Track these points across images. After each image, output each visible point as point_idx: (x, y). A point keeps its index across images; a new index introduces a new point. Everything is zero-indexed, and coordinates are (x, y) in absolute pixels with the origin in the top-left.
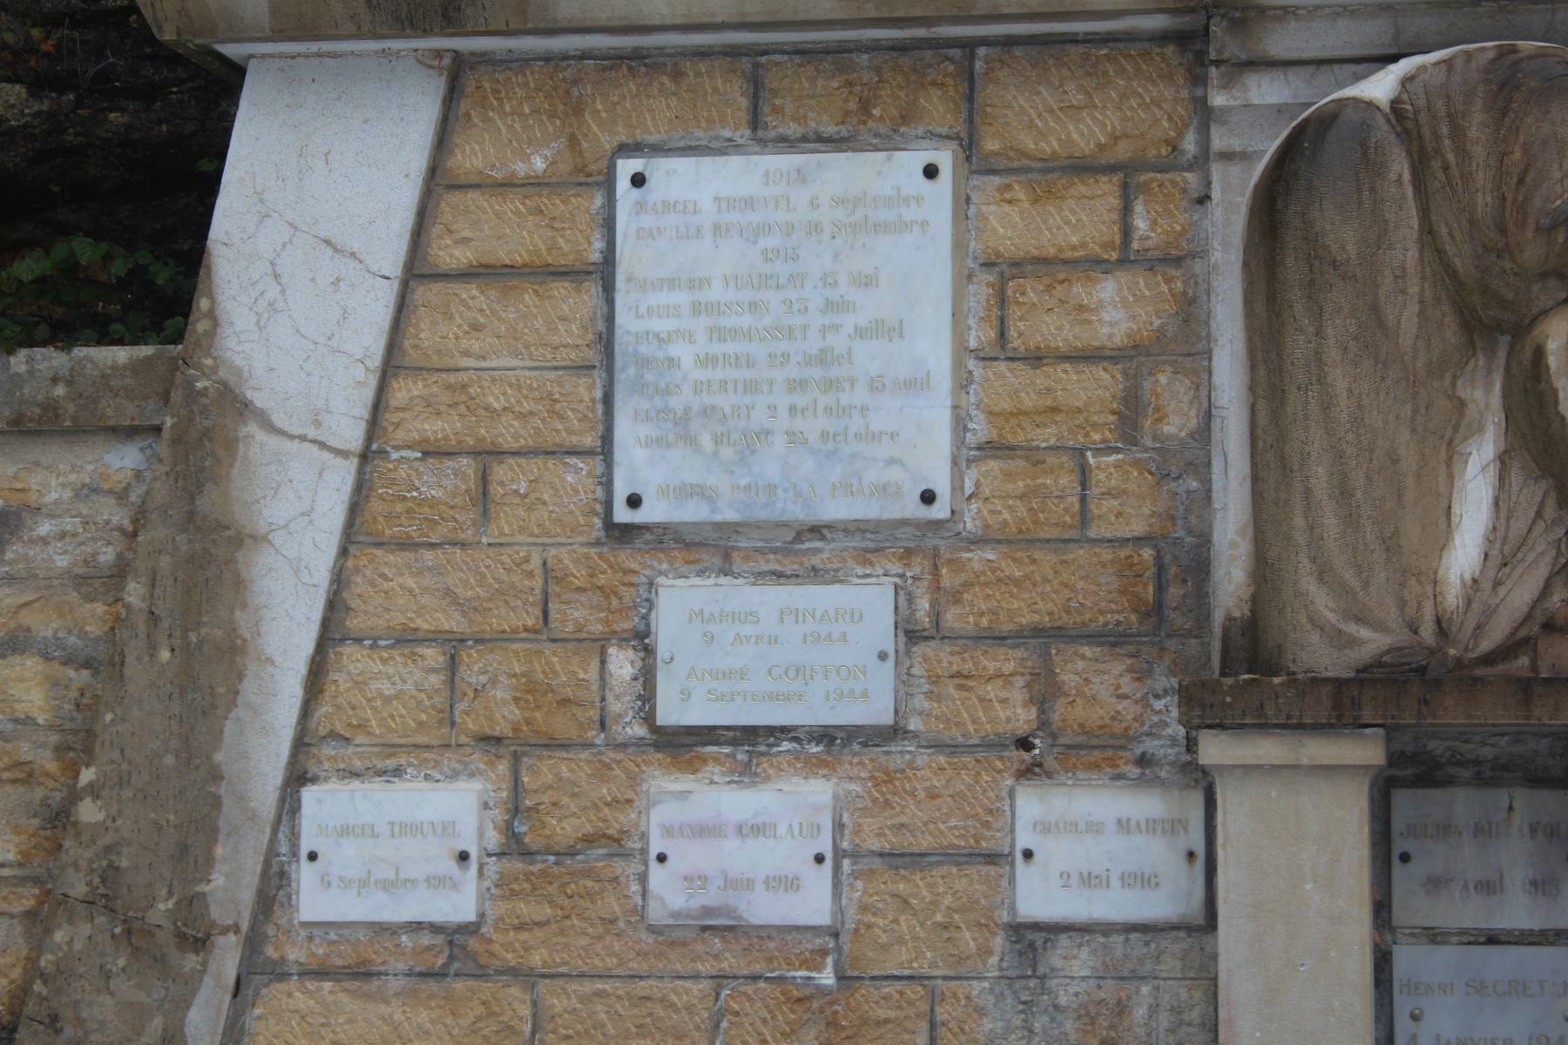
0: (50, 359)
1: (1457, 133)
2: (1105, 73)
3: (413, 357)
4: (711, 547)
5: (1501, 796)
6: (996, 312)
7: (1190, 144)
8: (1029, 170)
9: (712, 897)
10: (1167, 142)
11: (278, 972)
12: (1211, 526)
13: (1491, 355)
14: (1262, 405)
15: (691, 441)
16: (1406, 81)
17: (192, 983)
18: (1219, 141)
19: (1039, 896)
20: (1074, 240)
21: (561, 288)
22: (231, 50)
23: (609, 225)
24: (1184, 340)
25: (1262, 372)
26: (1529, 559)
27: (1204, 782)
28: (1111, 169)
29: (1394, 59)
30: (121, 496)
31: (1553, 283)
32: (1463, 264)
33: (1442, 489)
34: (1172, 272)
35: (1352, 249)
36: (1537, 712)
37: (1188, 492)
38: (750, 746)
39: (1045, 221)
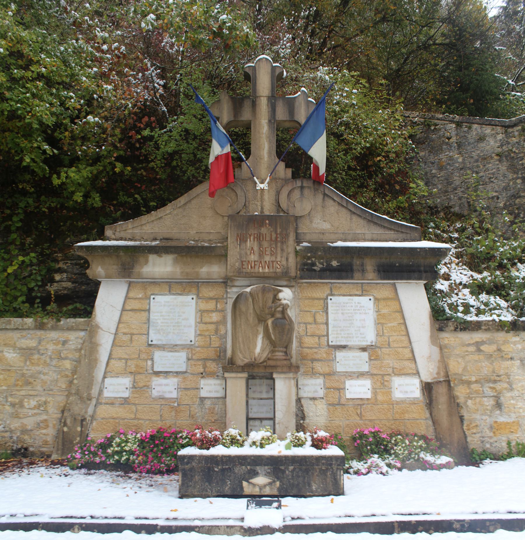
0: (72, 320)
1: (258, 296)
3: (122, 321)
4: (162, 347)
5: (262, 380)
7: (225, 296)
9: (160, 394)
11: (101, 404)
15: (160, 333)
17: (89, 405)
18: (229, 296)
19: (203, 393)
21: (143, 312)
22: (99, 280)
23: (149, 304)
24: (224, 321)
27: (225, 379)
30: (82, 339)
32: (258, 312)
38: (166, 374)
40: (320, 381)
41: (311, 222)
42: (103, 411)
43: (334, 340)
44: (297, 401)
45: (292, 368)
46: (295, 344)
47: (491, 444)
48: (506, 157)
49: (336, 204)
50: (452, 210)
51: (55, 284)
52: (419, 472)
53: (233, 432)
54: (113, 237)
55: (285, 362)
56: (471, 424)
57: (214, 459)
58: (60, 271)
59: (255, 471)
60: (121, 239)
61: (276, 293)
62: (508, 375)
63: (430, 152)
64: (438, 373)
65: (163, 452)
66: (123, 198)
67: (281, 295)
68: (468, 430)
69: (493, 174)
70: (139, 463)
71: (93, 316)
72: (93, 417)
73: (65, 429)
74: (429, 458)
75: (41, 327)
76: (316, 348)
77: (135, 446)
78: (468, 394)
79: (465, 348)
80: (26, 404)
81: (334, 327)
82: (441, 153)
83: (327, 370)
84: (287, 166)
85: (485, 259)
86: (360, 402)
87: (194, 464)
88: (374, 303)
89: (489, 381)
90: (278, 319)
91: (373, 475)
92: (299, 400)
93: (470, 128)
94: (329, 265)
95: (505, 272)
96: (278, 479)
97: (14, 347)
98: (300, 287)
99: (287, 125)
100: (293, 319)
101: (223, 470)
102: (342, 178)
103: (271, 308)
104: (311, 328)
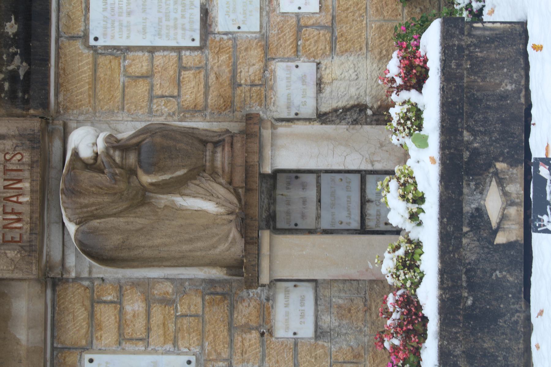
1: (86, 206)
2: (64, 308)
5: (279, 197)
6: (134, 341)
7: (86, 283)
8: (92, 331)
10: (85, 290)
12: (199, 279)
13: (152, 198)
14: (164, 264)
16: (70, 220)
18: (85, 275)
19: (307, 331)
20: (113, 318)
24: (145, 287)
25: (155, 264)
26: (211, 188)
27: (274, 282)
28: (92, 306)
29: (63, 224)
31: (131, 180)
32: (125, 205)
33: (190, 212)
34: (124, 288)
35: (119, 237)
36: (255, 187)
37: (189, 285)
39: (107, 326)
40: (280, 69)
43: (188, 35)
44: (323, 122)
45: (252, 130)
46: (199, 124)
53: (388, 264)
55: (238, 145)
57: (446, 308)
59: (472, 216)
61: (80, 164)
67: (86, 153)
76: (207, 77)
81: (159, 35)
83: (256, 54)
87: (458, 352)
90: (139, 161)
94: (15, 40)
96: (491, 165)
98: (66, 109)
101: (471, 287)
103: (114, 175)
104: (163, 86)
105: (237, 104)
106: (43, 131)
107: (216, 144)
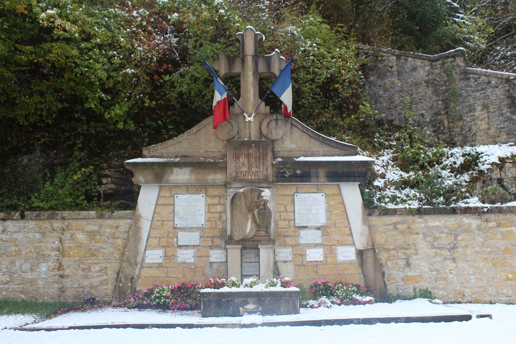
0: (122, 212)
4: (183, 229)
9: (183, 260)
11: (144, 267)
17: (136, 268)
18: (228, 194)
19: (212, 260)
24: (224, 211)
32: (248, 205)
38: (186, 247)
40: (289, 250)
41: (283, 143)
42: (145, 272)
43: (299, 222)
44: (274, 263)
45: (271, 241)
47: (403, 290)
48: (431, 84)
49: (300, 131)
50: (394, 123)
51: (103, 186)
52: (351, 306)
53: (233, 279)
54: (148, 155)
55: (266, 238)
56: (390, 277)
57: (222, 294)
58: (106, 176)
59: (247, 301)
60: (154, 157)
62: (415, 245)
63: (378, 77)
64: (367, 244)
65: (187, 297)
66: (149, 122)
67: (263, 194)
68: (388, 281)
69: (422, 96)
70: (172, 303)
71: (137, 209)
72: (138, 276)
73: (121, 285)
74: (358, 297)
75: (101, 217)
76: (287, 228)
77: (169, 293)
78: (388, 257)
79: (386, 227)
80: (92, 269)
82: (386, 79)
83: (294, 242)
84: (266, 105)
85: (412, 162)
86: (316, 264)
87: (210, 297)
88: (325, 198)
89: (402, 248)
91: (322, 308)
92: (275, 263)
93: (406, 60)
95: (425, 171)
96: (261, 305)
97: (83, 231)
98: (276, 187)
99: (266, 75)
100: (271, 209)
101: (228, 301)
102: (309, 103)
104: (284, 215)
105: (279, 237)
106: (269, 182)
107: (266, 231)
